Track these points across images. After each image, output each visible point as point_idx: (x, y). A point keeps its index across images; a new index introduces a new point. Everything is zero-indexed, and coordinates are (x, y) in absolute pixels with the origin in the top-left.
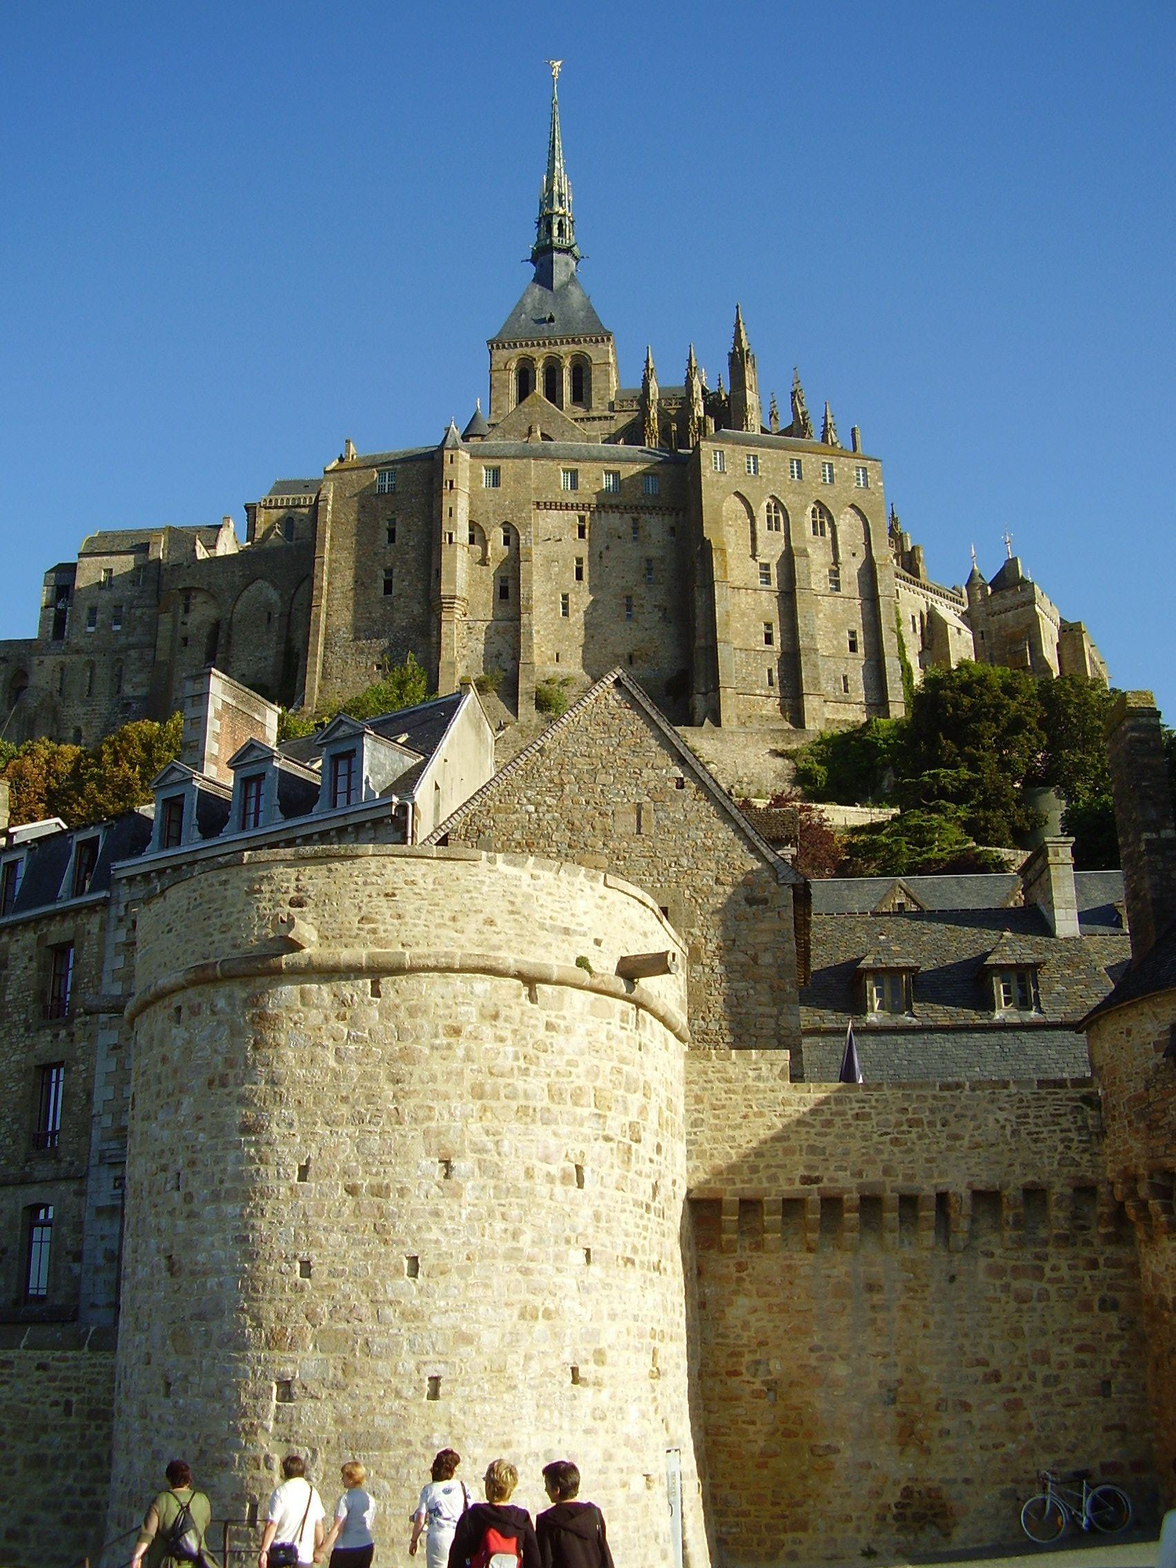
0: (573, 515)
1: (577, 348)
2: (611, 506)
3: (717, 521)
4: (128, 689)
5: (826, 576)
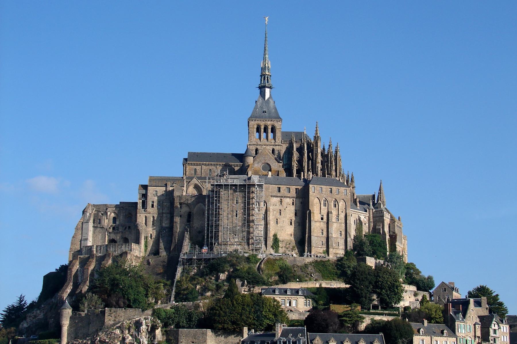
0: (279, 199)
1: (272, 123)
2: (288, 197)
3: (312, 205)
4: (164, 225)
5: (336, 218)
